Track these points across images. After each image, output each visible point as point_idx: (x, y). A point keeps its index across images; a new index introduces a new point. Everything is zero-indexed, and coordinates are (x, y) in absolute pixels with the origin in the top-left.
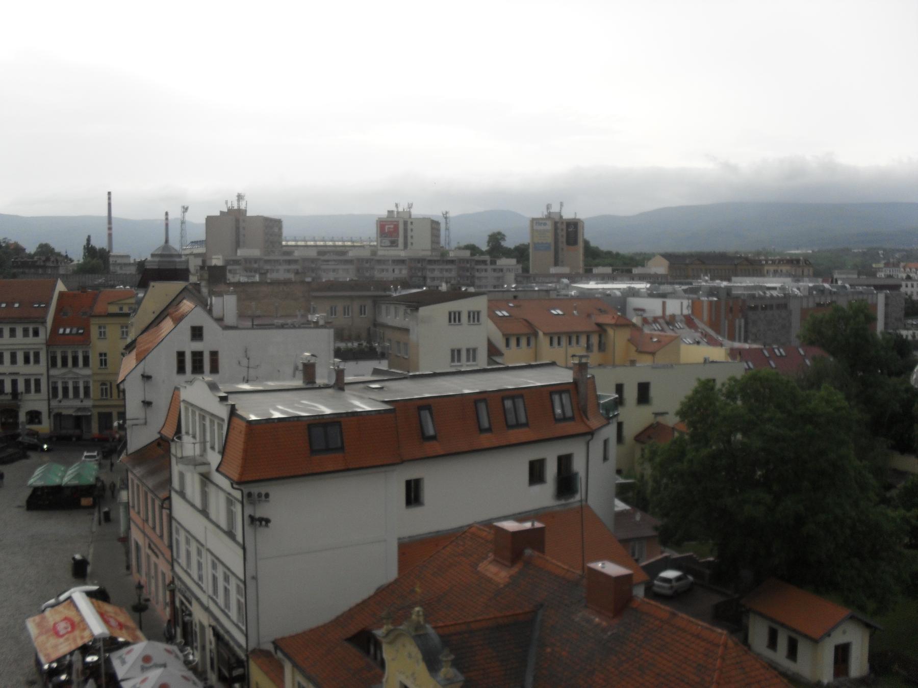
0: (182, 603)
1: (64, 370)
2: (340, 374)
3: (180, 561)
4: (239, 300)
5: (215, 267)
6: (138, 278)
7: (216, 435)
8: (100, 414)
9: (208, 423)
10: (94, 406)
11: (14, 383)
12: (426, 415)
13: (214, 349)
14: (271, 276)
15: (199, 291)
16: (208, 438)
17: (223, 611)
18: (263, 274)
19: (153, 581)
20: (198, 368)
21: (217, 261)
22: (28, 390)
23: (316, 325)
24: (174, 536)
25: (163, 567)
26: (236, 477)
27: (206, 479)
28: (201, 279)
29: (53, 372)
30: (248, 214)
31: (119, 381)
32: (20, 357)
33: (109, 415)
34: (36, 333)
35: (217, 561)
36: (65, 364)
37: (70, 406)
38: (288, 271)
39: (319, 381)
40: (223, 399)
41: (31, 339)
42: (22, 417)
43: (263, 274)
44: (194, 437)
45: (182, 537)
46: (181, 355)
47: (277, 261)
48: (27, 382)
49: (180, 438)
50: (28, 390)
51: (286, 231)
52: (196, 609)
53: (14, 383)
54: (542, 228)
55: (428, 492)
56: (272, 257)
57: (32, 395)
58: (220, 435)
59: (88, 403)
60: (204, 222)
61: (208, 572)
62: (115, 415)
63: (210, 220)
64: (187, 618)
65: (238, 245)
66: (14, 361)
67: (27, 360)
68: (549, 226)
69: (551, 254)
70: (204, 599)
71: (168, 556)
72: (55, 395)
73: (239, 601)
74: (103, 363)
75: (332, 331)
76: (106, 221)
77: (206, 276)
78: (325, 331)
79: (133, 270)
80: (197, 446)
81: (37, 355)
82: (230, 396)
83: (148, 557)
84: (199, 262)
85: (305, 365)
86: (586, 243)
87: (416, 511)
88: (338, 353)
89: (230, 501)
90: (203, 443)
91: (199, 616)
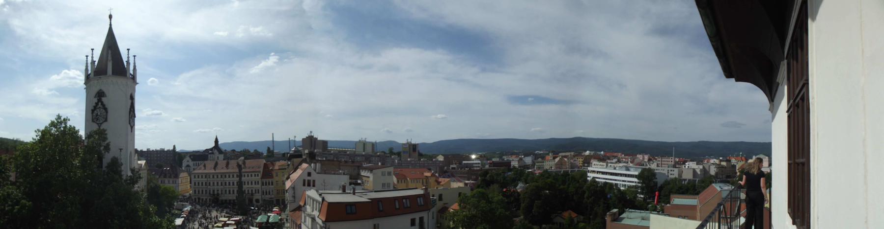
1: (266, 186)
2: (354, 190)
9: (315, 202)
11: (252, 190)
13: (314, 179)
14: (328, 158)
20: (309, 185)
22: (256, 193)
23: (344, 174)
26: (324, 220)
27: (313, 219)
29: (263, 187)
32: (254, 183)
37: (267, 197)
41: (257, 177)
42: (254, 202)
43: (326, 158)
44: (310, 206)
48: (256, 190)
50: (256, 193)
51: (329, 145)
53: (252, 190)
54: (406, 146)
57: (257, 194)
58: (319, 206)
59: (273, 196)
66: (252, 184)
67: (255, 184)
68: (407, 146)
69: (408, 154)
72: (263, 194)
75: (349, 176)
78: (347, 176)
81: (258, 182)
82: (323, 195)
86: (419, 152)
90: (313, 208)
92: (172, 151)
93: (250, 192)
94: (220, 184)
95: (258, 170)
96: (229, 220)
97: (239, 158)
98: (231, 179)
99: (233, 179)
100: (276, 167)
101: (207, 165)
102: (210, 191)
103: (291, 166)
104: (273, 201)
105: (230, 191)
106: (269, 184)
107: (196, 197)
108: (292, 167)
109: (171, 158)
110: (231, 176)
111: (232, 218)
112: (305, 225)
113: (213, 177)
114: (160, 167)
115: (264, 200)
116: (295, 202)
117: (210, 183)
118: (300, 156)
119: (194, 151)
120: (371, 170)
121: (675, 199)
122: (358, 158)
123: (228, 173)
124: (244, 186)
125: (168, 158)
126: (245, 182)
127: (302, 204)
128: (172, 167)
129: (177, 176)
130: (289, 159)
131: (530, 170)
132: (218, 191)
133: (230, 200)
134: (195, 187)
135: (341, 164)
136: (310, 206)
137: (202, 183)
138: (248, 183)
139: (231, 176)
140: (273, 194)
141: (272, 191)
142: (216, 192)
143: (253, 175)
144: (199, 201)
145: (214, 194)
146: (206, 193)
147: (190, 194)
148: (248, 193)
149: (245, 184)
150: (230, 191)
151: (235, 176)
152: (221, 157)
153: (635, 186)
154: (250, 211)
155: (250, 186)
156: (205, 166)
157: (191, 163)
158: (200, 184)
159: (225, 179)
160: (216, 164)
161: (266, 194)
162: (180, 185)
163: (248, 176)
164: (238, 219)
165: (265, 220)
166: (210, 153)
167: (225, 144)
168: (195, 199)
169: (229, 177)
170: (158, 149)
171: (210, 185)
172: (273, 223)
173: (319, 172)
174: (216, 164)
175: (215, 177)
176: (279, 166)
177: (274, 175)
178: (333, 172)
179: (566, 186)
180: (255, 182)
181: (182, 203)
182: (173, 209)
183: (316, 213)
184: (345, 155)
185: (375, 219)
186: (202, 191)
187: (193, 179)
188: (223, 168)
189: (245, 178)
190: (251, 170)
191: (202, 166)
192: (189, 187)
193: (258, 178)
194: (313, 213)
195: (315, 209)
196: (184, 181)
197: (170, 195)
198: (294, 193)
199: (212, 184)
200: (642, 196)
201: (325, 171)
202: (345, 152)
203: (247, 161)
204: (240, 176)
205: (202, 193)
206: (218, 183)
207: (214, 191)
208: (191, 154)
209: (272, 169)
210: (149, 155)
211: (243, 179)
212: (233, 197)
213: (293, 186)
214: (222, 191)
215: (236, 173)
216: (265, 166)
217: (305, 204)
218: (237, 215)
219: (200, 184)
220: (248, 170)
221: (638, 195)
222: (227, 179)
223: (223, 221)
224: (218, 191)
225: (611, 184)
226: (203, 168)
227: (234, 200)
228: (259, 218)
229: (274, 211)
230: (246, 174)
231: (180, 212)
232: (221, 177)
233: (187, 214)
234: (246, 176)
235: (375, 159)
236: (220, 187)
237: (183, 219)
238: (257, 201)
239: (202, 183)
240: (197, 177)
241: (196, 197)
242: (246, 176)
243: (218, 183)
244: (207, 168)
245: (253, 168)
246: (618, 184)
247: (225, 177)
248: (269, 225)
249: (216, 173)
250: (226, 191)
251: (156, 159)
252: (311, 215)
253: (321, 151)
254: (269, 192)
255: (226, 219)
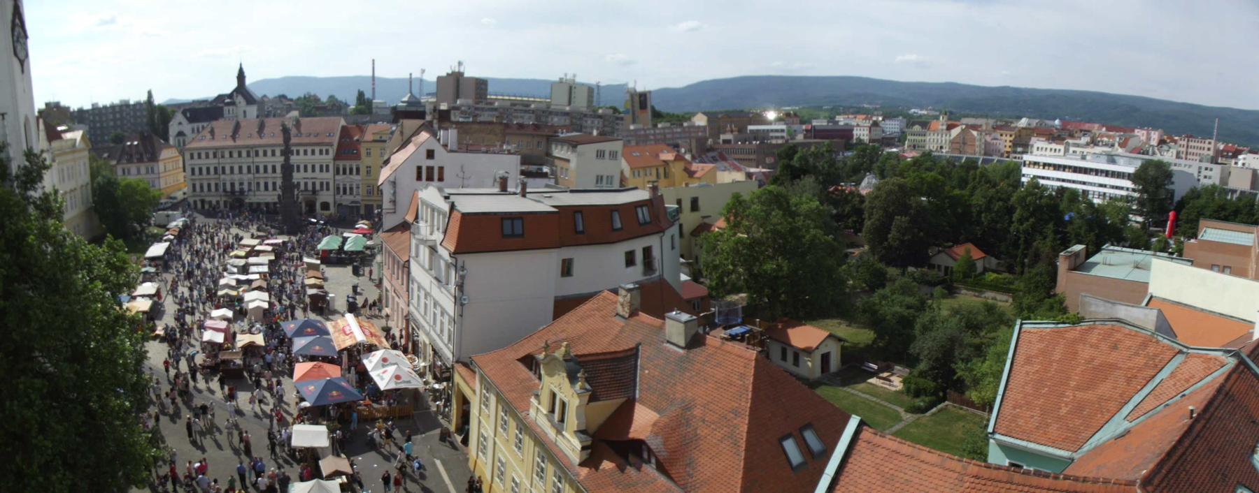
0: (413, 329)
1: (345, 176)
3: (413, 301)
4: (458, 132)
5: (443, 111)
6: (392, 117)
7: (440, 222)
8: (366, 206)
10: (362, 200)
11: (314, 184)
12: (579, 217)
13: (440, 165)
15: (432, 126)
16: (436, 223)
17: (438, 335)
18: (476, 116)
19: (396, 313)
20: (430, 178)
21: (444, 107)
22: (322, 189)
24: (411, 285)
25: (402, 305)
27: (433, 249)
28: (434, 118)
29: (337, 177)
30: (466, 75)
31: (379, 184)
33: (372, 206)
34: (327, 152)
35: (436, 304)
36: (344, 173)
37: (346, 199)
38: (491, 116)
39: (510, 189)
40: (447, 198)
41: (324, 156)
45: (415, 287)
46: (419, 168)
47: (483, 109)
48: (322, 184)
49: (417, 222)
50: (322, 189)
51: (490, 89)
52: (421, 333)
53: (314, 184)
55: (577, 268)
56: (480, 106)
59: (358, 198)
60: (435, 79)
61: (431, 309)
62: (375, 206)
63: (439, 79)
64: (416, 338)
65: (458, 97)
66: (313, 170)
67: (321, 170)
70: (427, 327)
71: (406, 300)
72: (338, 193)
73: (449, 330)
74: (368, 173)
76: (371, 79)
77: (437, 116)
79: (388, 112)
80: (428, 228)
81: (327, 167)
83: (393, 298)
84: (432, 107)
85: (501, 178)
87: (568, 279)
88: (523, 173)
89: (448, 266)
90: (432, 226)
91: (423, 338)
92: (145, 103)
93: (310, 187)
94: (245, 170)
95: (327, 140)
96: (260, 244)
97: (288, 112)
98: (269, 159)
99: (273, 159)
100: (369, 136)
101: (216, 130)
102: (224, 185)
103: (397, 134)
104: (358, 208)
105: (266, 185)
106: (351, 173)
107: (197, 199)
108: (400, 138)
109: (145, 120)
110: (269, 153)
111: (268, 238)
112: (418, 262)
113: (231, 155)
114: (119, 140)
115: (340, 205)
116: (395, 212)
117: (223, 169)
118: (420, 115)
119: (194, 102)
120: (573, 144)
121: (1209, 230)
122: (556, 119)
123: (260, 146)
124: (295, 174)
125: (139, 120)
126: (298, 167)
127: (410, 218)
128: (144, 139)
129: (154, 158)
130: (395, 121)
131: (894, 150)
132: (241, 184)
133: (267, 204)
134: (193, 177)
135: (508, 131)
136: (426, 222)
137: (208, 169)
138: (306, 167)
139: (269, 153)
140: (358, 195)
141: (358, 188)
142: (237, 188)
143: (317, 152)
144: (203, 207)
145: (233, 192)
146: (217, 189)
147: (184, 194)
148: (306, 190)
149: (298, 170)
150: (266, 185)
151: (278, 153)
152: (253, 111)
153: (1127, 196)
154: (308, 225)
155: (310, 174)
156: (212, 132)
157: (187, 128)
158: (204, 171)
159: (257, 159)
160: (237, 128)
161: (345, 193)
162: (161, 175)
163: (305, 153)
164: (279, 240)
165: (335, 246)
166: (228, 104)
167: (257, 83)
168: (195, 202)
169: (265, 154)
170: (116, 101)
171: (224, 172)
172: (352, 252)
173: (455, 148)
174: (237, 128)
175: (235, 155)
176: (374, 134)
177: (363, 152)
178: (484, 149)
179: (966, 192)
180: (321, 167)
181: (166, 212)
182: (150, 225)
183: (438, 236)
184: (526, 111)
185: (563, 248)
186: (209, 185)
187: (188, 162)
188: (251, 136)
189: (298, 157)
190: (315, 140)
191: (206, 133)
192: (182, 180)
193: (328, 159)
194: (433, 238)
195: (435, 228)
196: (169, 167)
197: (138, 197)
198: (394, 194)
199: (228, 170)
200: (1140, 219)
201: (468, 145)
202: (527, 104)
203: (305, 121)
204: (287, 152)
205: (209, 189)
206: (240, 168)
207: (232, 185)
208: (187, 107)
209: (358, 140)
210: (97, 118)
211: (294, 159)
212: (271, 197)
213: (392, 179)
214: (250, 184)
215: (279, 145)
216: (345, 131)
217: (417, 218)
218: (281, 233)
219: (204, 171)
220: (306, 140)
221: (1131, 216)
222: (260, 160)
223: (248, 246)
224: (241, 184)
225: (1074, 193)
226: (209, 136)
227: (275, 204)
228: (325, 240)
229: (357, 229)
230: (302, 150)
231: (161, 231)
232: (248, 155)
233: (176, 234)
234: (302, 152)
235: (593, 122)
236: (246, 177)
237: (168, 243)
238: (325, 206)
239: (208, 169)
240: (196, 156)
241: (197, 199)
242: (302, 152)
243: (240, 168)
244: (215, 137)
245: (316, 136)
246: (1088, 191)
247: (257, 154)
248: (343, 256)
249: (235, 147)
250: (258, 184)
251: (112, 124)
252: (427, 241)
253: (470, 102)
254: (351, 189)
255: (255, 242)
